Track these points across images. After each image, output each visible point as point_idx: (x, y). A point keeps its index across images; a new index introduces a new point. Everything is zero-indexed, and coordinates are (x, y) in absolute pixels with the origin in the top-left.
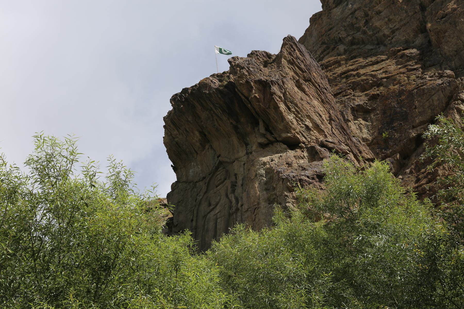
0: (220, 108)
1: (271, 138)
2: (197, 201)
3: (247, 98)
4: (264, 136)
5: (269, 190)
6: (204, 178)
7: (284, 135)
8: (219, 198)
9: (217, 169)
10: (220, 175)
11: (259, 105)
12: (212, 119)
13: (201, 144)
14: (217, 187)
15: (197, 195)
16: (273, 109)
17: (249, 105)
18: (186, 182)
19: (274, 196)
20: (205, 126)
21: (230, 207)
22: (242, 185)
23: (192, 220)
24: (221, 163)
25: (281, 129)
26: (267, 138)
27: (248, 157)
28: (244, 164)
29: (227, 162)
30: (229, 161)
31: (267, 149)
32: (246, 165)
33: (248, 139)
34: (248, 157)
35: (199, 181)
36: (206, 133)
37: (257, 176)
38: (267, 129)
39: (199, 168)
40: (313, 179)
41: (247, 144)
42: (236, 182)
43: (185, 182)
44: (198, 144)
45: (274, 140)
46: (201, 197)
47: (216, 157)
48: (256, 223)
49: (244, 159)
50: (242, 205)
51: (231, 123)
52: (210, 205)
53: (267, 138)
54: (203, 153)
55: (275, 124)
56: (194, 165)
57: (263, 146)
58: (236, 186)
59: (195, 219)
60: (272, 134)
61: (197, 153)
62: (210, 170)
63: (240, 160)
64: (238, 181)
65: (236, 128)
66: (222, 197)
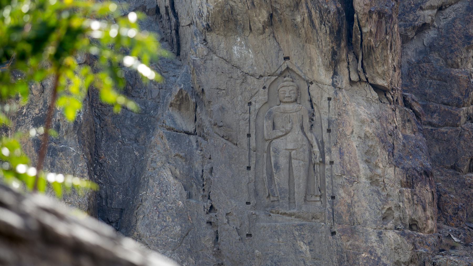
0: (330, 29)
1: (363, 78)
2: (252, 108)
4: (358, 72)
5: (369, 162)
6: (261, 76)
7: (380, 82)
8: (289, 125)
10: (286, 88)
11: (370, 40)
12: (292, 9)
13: (263, 26)
15: (251, 97)
16: (380, 50)
17: (360, 37)
18: (227, 62)
19: (378, 178)
20: (280, 12)
21: (311, 153)
22: (329, 131)
23: (249, 135)
24: (288, 68)
25: (378, 73)
26: (359, 76)
28: (329, 99)
29: (300, 76)
30: (303, 77)
31: (355, 88)
32: (332, 102)
33: (338, 67)
35: (252, 75)
36: (277, 19)
37: (354, 134)
38: (362, 66)
39: (249, 52)
40: (421, 174)
41: (335, 73)
42: (313, 115)
43: (225, 60)
44: (261, 26)
45: (366, 80)
46: (257, 106)
47: (282, 57)
48: (355, 202)
49: (330, 92)
50: (332, 163)
51: (333, 48)
52: (274, 127)
53: (359, 76)
54: (261, 37)
55: (375, 64)
56: (240, 42)
58: (313, 120)
59: (253, 136)
60: (364, 72)
61: (251, 29)
62: (273, 71)
63: (320, 85)
64: (317, 115)
65: (334, 53)
66: (294, 127)
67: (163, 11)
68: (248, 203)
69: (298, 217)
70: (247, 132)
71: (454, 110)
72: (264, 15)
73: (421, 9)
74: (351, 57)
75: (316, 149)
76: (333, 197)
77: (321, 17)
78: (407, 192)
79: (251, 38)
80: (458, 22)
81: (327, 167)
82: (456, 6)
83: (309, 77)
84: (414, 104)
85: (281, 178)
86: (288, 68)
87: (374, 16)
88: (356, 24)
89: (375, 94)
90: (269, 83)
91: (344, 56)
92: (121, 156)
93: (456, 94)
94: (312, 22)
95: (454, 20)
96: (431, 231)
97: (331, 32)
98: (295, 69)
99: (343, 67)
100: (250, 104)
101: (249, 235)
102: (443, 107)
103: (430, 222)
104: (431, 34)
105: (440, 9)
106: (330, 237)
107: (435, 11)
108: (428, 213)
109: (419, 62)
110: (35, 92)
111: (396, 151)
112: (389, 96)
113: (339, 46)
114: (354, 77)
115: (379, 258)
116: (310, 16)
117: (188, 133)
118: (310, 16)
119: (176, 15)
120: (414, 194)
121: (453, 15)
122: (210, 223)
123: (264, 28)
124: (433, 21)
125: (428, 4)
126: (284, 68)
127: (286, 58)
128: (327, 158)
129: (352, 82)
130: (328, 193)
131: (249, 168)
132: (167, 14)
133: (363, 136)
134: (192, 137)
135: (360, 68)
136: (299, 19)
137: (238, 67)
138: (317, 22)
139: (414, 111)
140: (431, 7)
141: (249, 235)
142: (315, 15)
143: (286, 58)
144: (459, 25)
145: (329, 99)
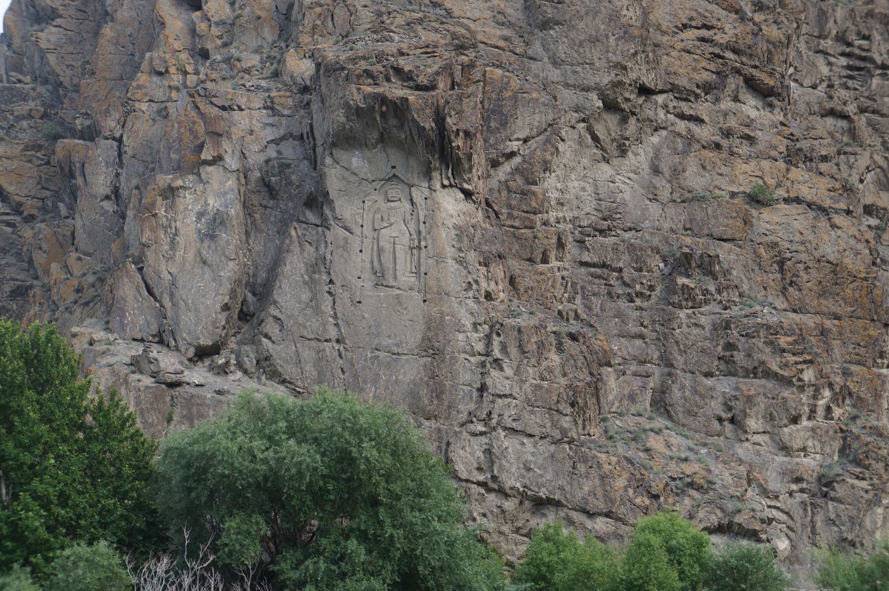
3: (450, 142)
7: (466, 186)
9: (388, 180)
14: (388, 201)
23: (362, 226)
24: (394, 175)
27: (431, 194)
31: (446, 190)
32: (428, 201)
34: (431, 194)
36: (386, 136)
38: (453, 174)
50: (426, 247)
54: (375, 151)
57: (444, 186)
60: (454, 178)
67: (305, 136)
68: (359, 278)
69: (399, 289)
70: (361, 223)
71: (532, 216)
72: (375, 135)
73: (510, 140)
74: (443, 167)
75: (415, 236)
76: (426, 274)
77: (419, 133)
78: (483, 269)
79: (366, 152)
80: (538, 150)
81: (423, 251)
82: (537, 139)
83: (411, 181)
84: (493, 204)
85: (387, 259)
86: (394, 175)
87: (461, 134)
88: (446, 139)
89: (462, 196)
90: (379, 186)
91: (437, 165)
92: (265, 244)
93: (534, 204)
94: (413, 138)
95: (535, 150)
96: (502, 301)
97: (427, 146)
98: (400, 175)
99: (436, 175)
100: (364, 202)
101: (360, 302)
102: (523, 214)
103: (501, 294)
104: (517, 160)
105: (525, 141)
106: (422, 304)
107: (521, 142)
108: (500, 287)
109: (507, 181)
110: (198, 193)
111: (476, 239)
112: (474, 198)
113: (433, 156)
114: (446, 182)
115: (459, 320)
116: (411, 133)
117: (317, 226)
118: (411, 133)
119: (314, 139)
120: (488, 271)
121: (534, 146)
122: (329, 293)
123: (377, 143)
124: (519, 150)
125: (515, 136)
126: (391, 175)
127: (394, 167)
128: (423, 243)
129: (444, 186)
130: (423, 270)
131: (361, 251)
132: (308, 138)
133: (450, 225)
134: (320, 229)
135: (450, 175)
136: (403, 136)
137: (355, 174)
138: (416, 138)
139: (494, 210)
140: (518, 139)
141: (360, 302)
142: (415, 132)
143: (394, 167)
144: (538, 153)
145: (426, 199)
